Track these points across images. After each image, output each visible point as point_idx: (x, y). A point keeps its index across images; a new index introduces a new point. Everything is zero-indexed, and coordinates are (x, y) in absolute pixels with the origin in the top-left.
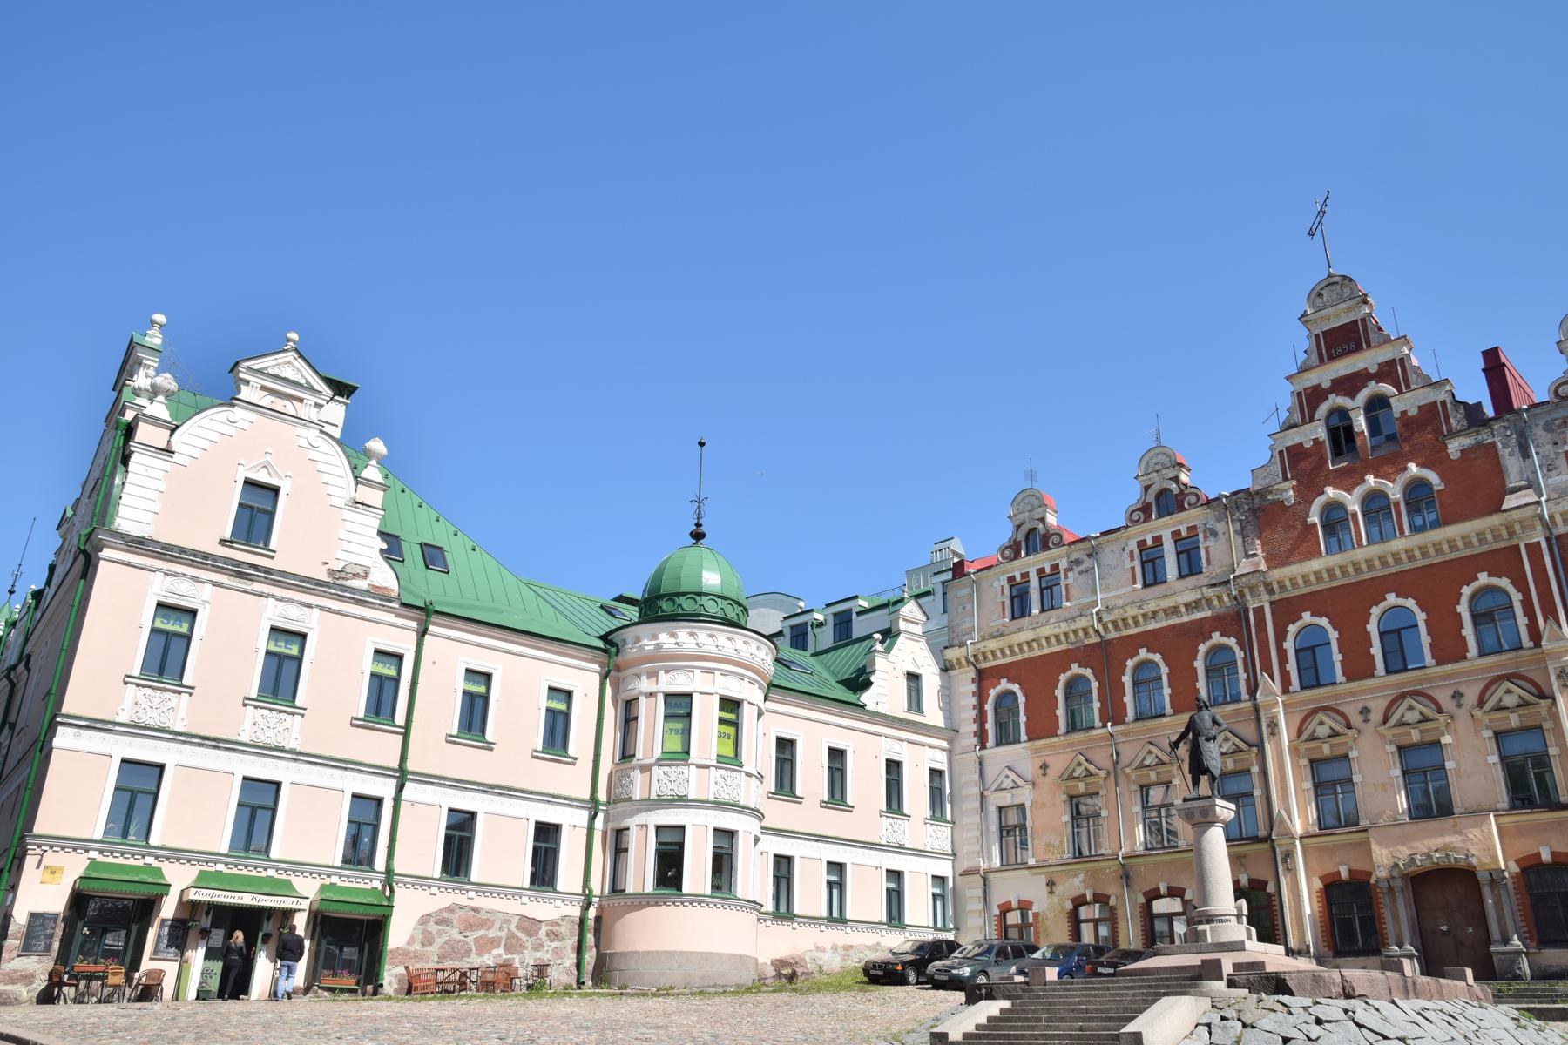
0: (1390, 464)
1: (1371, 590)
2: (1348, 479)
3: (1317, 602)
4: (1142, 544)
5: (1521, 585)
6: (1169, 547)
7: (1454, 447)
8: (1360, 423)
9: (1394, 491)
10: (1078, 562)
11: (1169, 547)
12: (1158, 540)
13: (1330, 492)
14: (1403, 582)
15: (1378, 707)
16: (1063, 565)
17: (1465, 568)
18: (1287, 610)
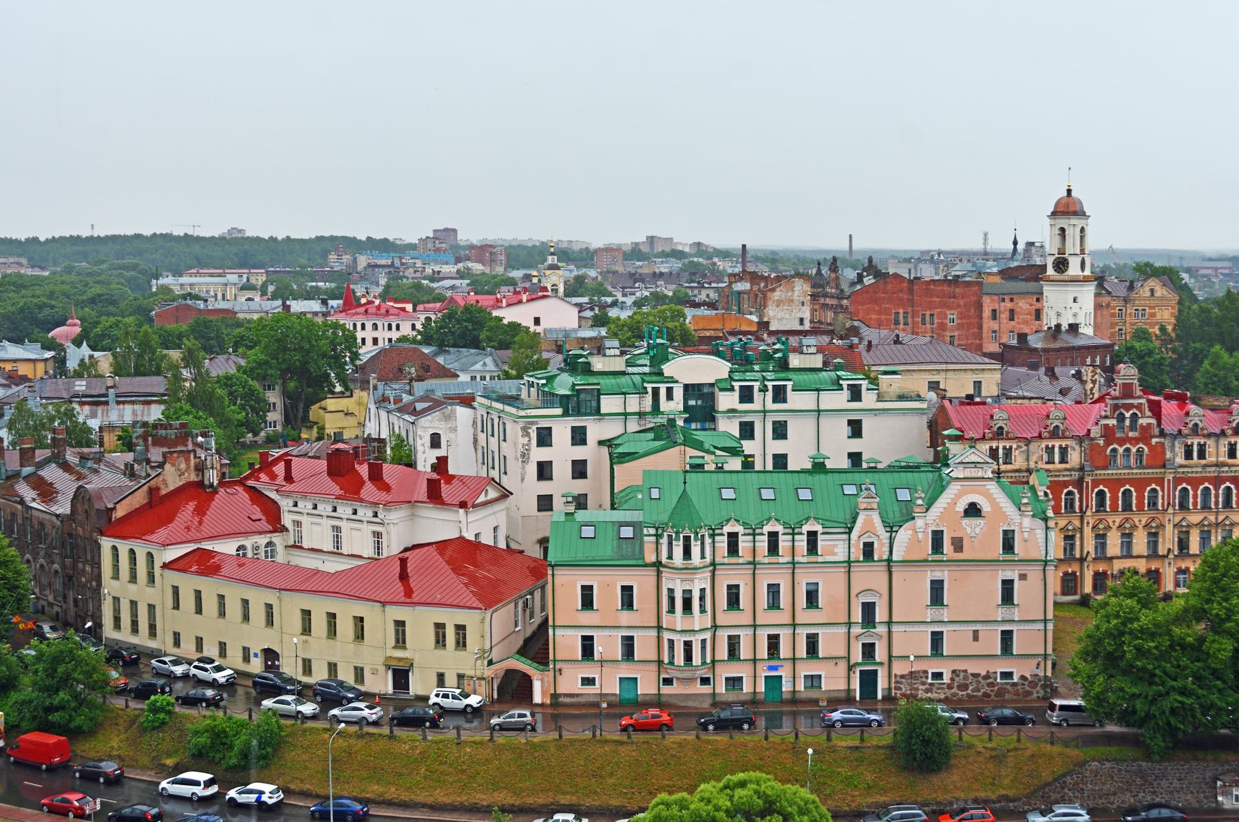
0: (1135, 441)
1: (1122, 482)
2: (1121, 442)
3: (1105, 482)
4: (1047, 447)
5: (1163, 491)
6: (1057, 450)
7: (1154, 441)
8: (1127, 422)
9: (1134, 450)
10: (1019, 447)
11: (1057, 450)
12: (1053, 447)
13: (1115, 446)
14: (1130, 481)
15: (1118, 520)
16: (1014, 446)
17: (1148, 481)
18: (1096, 483)
